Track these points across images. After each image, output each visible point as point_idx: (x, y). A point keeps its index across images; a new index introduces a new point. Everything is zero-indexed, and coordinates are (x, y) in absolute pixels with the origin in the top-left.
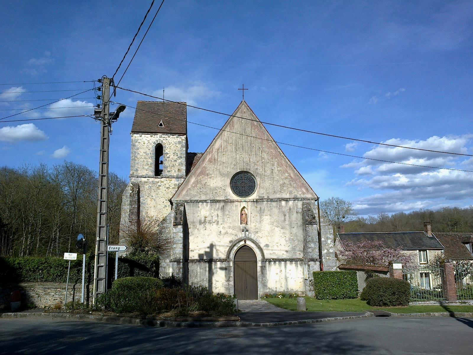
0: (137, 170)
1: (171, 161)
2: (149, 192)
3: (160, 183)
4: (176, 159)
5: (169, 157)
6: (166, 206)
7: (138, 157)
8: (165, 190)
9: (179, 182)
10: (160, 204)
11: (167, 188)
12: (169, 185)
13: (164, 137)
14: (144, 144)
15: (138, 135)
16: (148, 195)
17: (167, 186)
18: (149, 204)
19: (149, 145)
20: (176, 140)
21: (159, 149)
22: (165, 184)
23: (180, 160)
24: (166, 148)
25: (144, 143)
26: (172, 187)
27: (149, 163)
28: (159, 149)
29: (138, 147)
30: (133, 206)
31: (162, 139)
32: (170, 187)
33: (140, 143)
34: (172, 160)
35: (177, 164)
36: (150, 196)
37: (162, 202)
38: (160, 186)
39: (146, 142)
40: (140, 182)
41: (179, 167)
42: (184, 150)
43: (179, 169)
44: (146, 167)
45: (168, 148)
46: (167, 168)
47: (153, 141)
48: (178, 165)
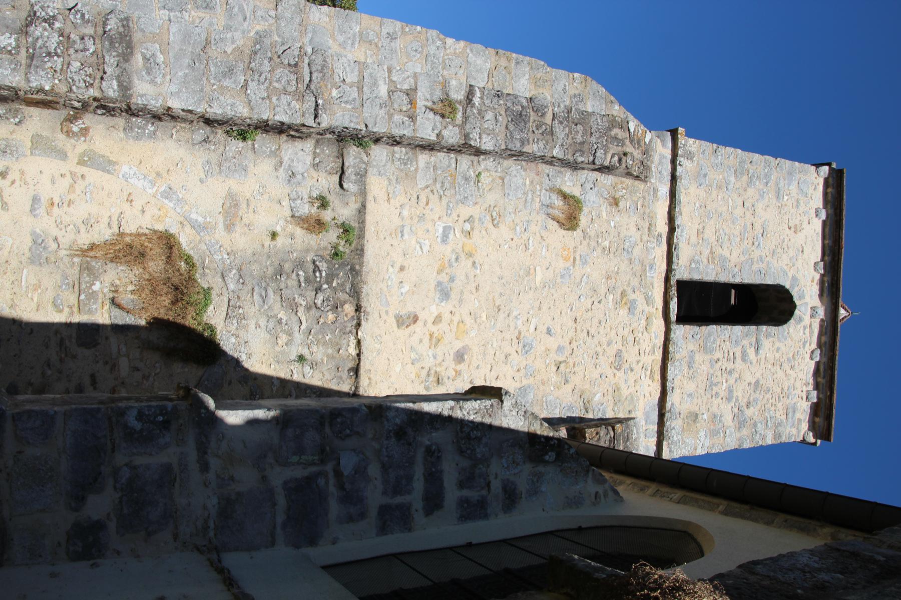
0: (700, 176)
1: (730, 373)
2: (606, 243)
3: (647, 309)
4: (737, 400)
5: (744, 355)
6: (527, 348)
7: (751, 191)
8: (609, 344)
9: (642, 423)
10: (545, 308)
11: (618, 354)
12: (634, 366)
13: (811, 333)
14: (793, 229)
15: (820, 204)
16: (592, 233)
17: (630, 355)
18: (544, 233)
19: (791, 253)
20: (798, 392)
21: (761, 305)
22: (638, 343)
23: (731, 417)
24: (777, 344)
25: (795, 226)
26: (623, 386)
27: (725, 252)
28: (761, 305)
29: (786, 198)
30: (561, 132)
31: (807, 319)
32: (619, 374)
33: (797, 207)
34: (736, 375)
35: (716, 401)
36: (585, 243)
37: (549, 323)
38: (632, 308)
39: (800, 238)
40: (655, 191)
41: (705, 416)
42: (764, 438)
43: (696, 416)
44: (709, 234)
45: (778, 349)
46: (705, 352)
47: (799, 276)
48: (714, 409)
